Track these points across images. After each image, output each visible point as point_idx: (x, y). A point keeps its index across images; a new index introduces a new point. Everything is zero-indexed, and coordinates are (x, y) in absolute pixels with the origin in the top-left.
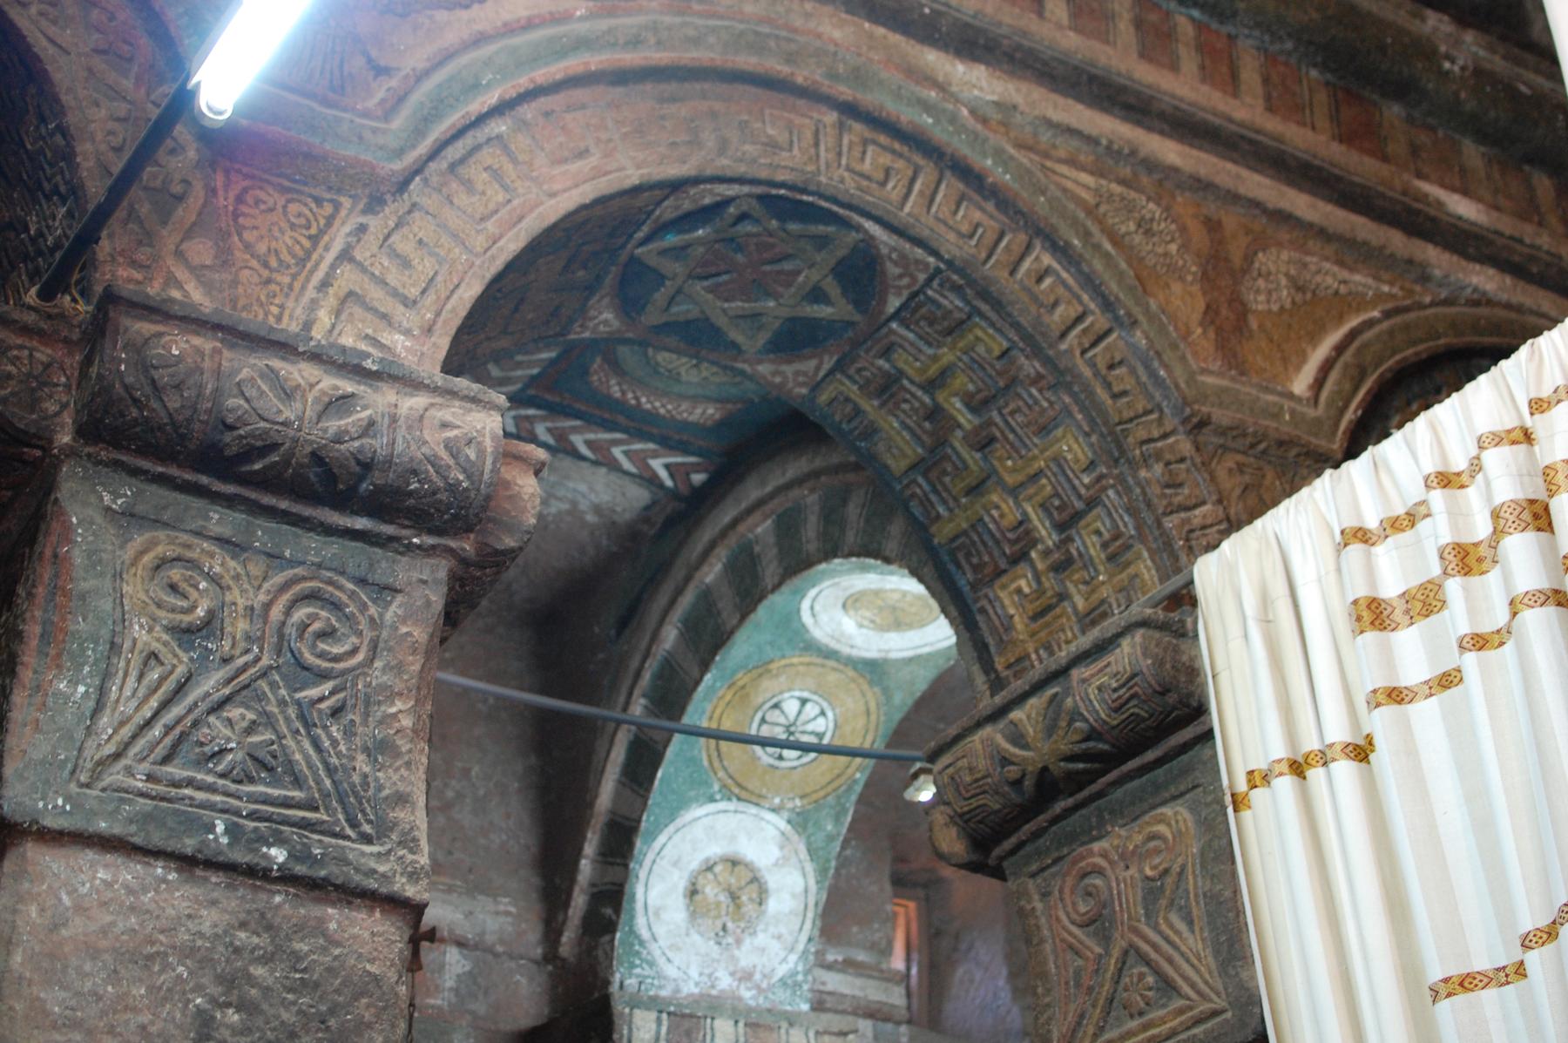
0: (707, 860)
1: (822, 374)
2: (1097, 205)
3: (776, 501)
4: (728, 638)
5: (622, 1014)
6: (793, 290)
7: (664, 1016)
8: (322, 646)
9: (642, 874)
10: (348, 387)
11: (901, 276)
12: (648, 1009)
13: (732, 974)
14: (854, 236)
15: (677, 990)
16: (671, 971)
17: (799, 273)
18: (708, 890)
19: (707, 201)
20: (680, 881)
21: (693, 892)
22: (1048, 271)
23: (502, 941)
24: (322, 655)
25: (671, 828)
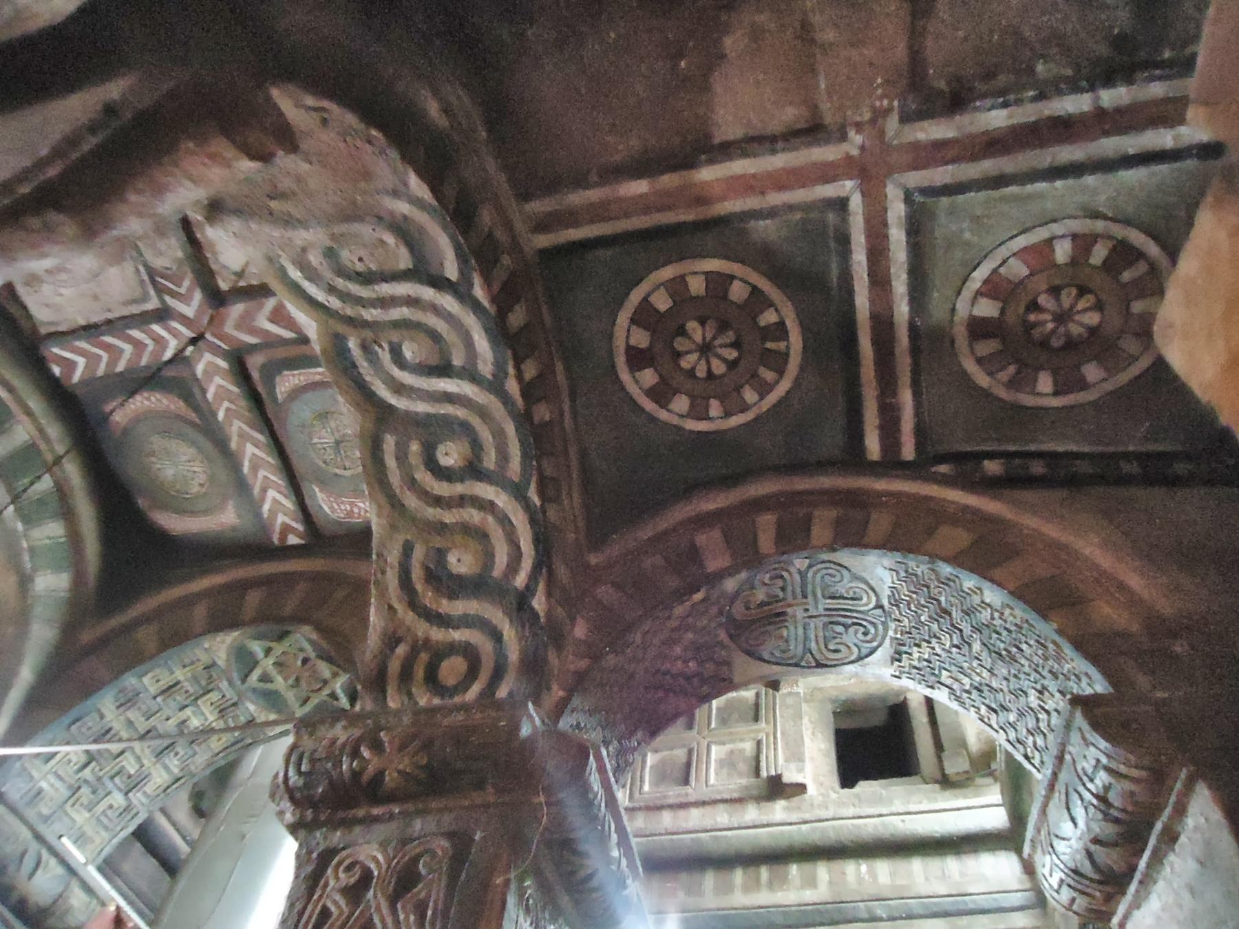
17: (285, 679)
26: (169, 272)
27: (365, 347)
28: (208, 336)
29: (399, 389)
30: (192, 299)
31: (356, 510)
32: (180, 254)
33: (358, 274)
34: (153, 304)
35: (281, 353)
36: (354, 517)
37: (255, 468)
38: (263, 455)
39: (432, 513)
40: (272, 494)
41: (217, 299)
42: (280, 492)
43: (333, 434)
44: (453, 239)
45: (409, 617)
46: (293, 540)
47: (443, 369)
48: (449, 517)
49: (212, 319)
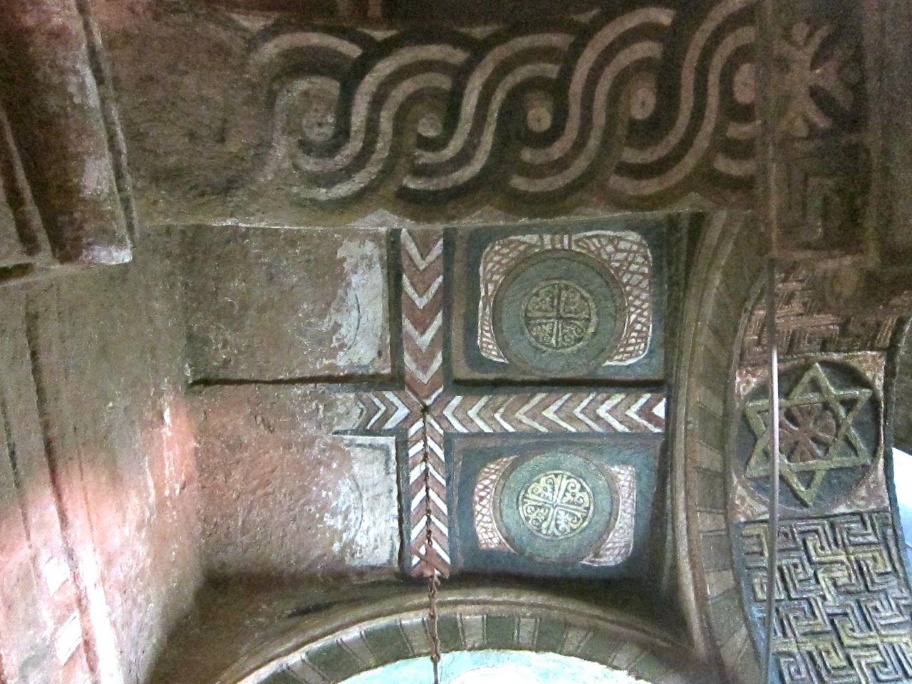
1: (761, 518)
3: (502, 607)
4: (414, 656)
6: (801, 463)
11: (863, 498)
14: (869, 462)
17: (814, 457)
19: (869, 375)
26: (365, 413)
27: (419, 172)
28: (428, 402)
29: (464, 157)
30: (392, 403)
31: (638, 327)
32: (352, 396)
33: (335, 136)
34: (390, 441)
35: (457, 336)
36: (647, 332)
37: (571, 419)
38: (559, 403)
39: (593, 142)
40: (602, 411)
41: (397, 381)
42: (603, 403)
43: (549, 318)
44: (315, 29)
45: (690, 161)
46: (660, 410)
47: (451, 107)
48: (600, 119)
49: (411, 389)
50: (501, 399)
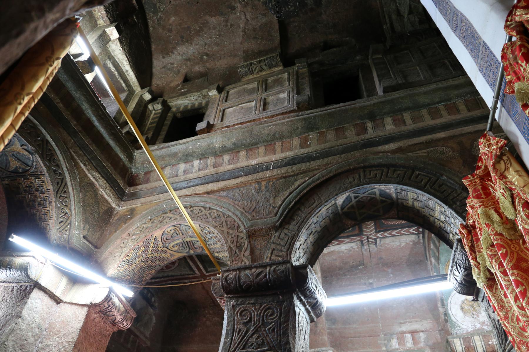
0: (462, 301)
2: (428, 155)
5: (451, 341)
7: (461, 339)
8: (270, 318)
9: (449, 308)
10: (259, 270)
12: (457, 338)
13: (479, 324)
15: (467, 331)
16: (464, 327)
18: (465, 307)
20: (459, 307)
21: (462, 309)
22: (419, 174)
23: (431, 329)
24: (271, 319)
25: (451, 297)
50: (364, 227)
